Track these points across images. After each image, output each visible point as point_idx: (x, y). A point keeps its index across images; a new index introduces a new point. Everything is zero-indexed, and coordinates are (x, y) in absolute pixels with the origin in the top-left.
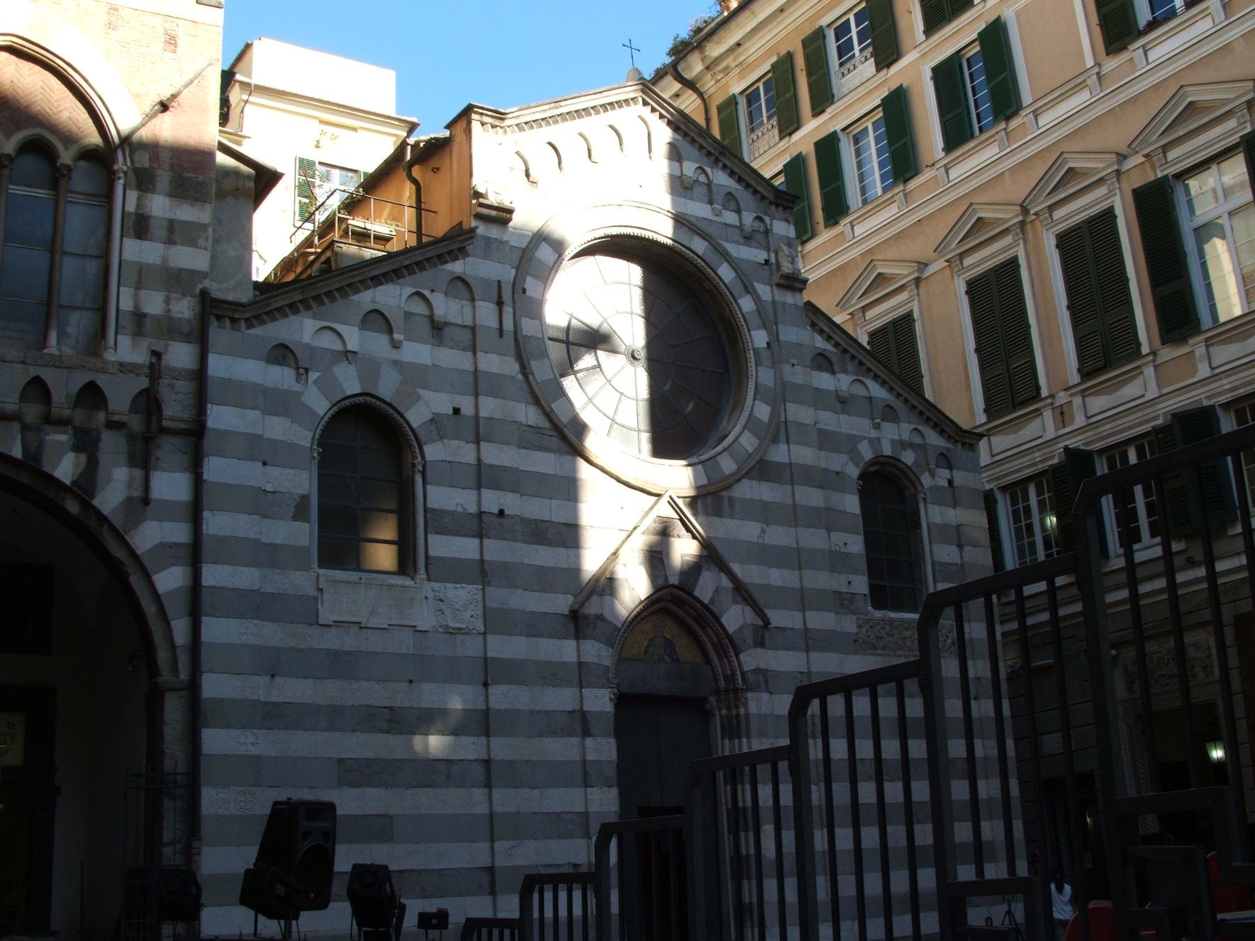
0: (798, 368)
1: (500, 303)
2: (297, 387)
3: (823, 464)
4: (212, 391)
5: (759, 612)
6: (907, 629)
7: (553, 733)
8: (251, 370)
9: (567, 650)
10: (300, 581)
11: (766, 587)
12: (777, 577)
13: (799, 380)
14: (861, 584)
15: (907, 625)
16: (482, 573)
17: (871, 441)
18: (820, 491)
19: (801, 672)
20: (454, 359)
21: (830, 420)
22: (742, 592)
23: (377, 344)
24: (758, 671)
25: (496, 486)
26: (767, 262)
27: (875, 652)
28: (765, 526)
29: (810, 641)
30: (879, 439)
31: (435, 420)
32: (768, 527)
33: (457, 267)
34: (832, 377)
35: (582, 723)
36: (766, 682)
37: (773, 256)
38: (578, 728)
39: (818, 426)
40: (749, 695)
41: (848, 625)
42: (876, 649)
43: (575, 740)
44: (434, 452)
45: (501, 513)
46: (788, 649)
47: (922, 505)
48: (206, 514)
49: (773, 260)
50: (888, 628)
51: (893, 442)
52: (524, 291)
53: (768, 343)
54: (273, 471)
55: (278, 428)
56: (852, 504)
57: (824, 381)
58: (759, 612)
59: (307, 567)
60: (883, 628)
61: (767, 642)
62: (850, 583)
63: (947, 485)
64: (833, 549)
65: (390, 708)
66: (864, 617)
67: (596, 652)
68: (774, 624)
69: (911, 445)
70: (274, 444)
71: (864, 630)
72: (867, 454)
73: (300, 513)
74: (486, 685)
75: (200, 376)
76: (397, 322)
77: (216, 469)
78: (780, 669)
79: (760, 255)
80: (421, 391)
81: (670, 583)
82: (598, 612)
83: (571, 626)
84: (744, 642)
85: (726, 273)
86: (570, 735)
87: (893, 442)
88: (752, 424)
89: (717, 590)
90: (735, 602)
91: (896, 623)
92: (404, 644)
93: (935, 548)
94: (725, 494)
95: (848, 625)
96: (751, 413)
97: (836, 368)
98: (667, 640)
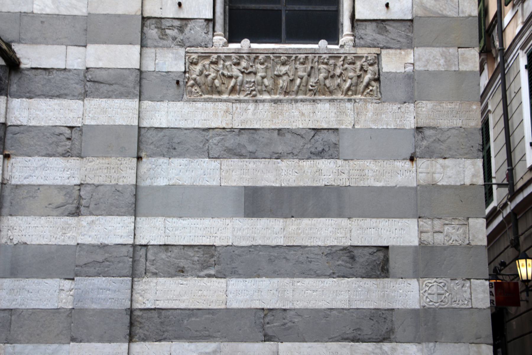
6: (284, 64)
15: (283, 58)
19: (71, 128)
27: (215, 97)
29: (88, 84)
42: (220, 93)
46: (52, 97)
50: (244, 64)
60: (237, 64)
61: (14, 88)
62: (180, 4)
66: (200, 50)
68: (25, 64)
71: (198, 68)
78: (33, 123)
91: (261, 57)
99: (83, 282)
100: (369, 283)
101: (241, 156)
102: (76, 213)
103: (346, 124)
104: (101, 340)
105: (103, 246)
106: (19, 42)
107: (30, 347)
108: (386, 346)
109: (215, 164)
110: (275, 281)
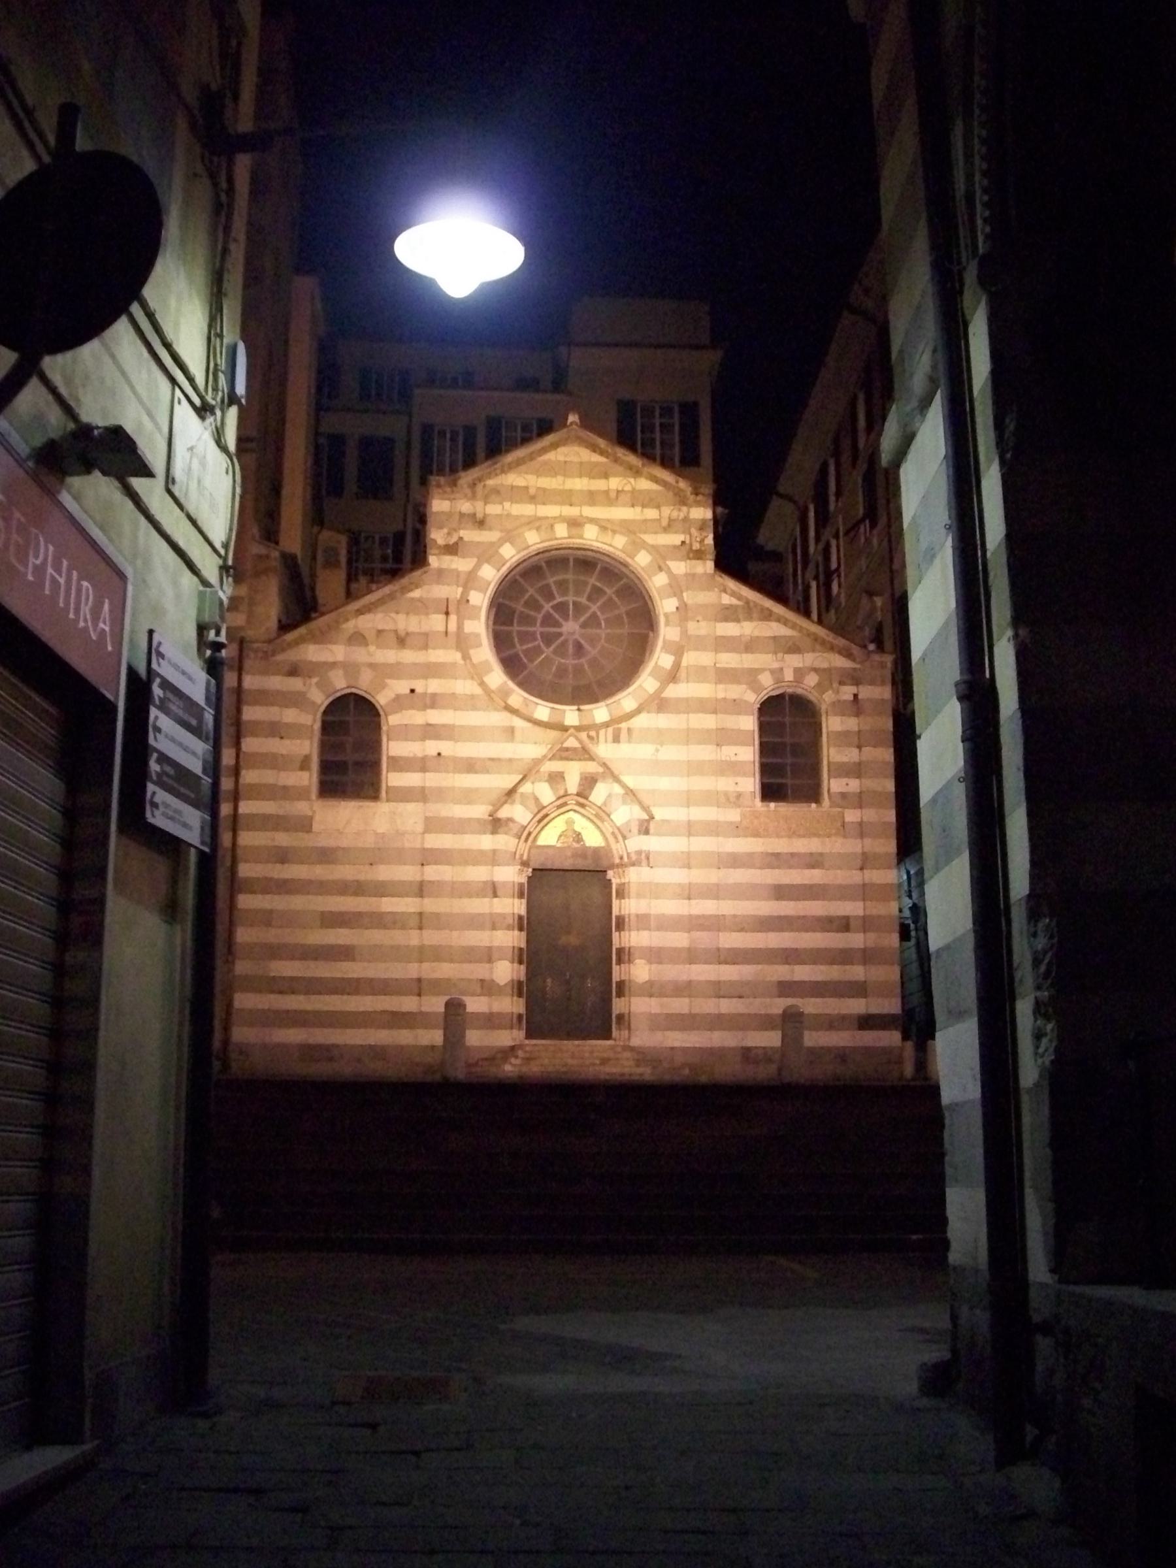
0: (703, 624)
1: (447, 613)
2: (303, 689)
3: (721, 695)
4: (244, 697)
5: (646, 809)
7: (470, 896)
8: (276, 682)
9: (486, 842)
10: (301, 808)
11: (653, 792)
12: (665, 783)
13: (703, 632)
14: (750, 784)
16: (421, 795)
17: (772, 672)
18: (714, 716)
20: (409, 656)
21: (729, 660)
22: (631, 794)
23: (360, 655)
24: (639, 853)
25: (437, 737)
26: (683, 543)
28: (659, 747)
30: (782, 669)
31: (398, 698)
32: (662, 746)
33: (416, 594)
34: (738, 625)
35: (494, 890)
36: (648, 859)
37: (688, 537)
38: (490, 893)
39: (717, 665)
40: (632, 869)
41: (734, 815)
43: (486, 900)
44: (392, 720)
45: (439, 754)
47: (824, 719)
48: (243, 772)
49: (688, 542)
51: (797, 671)
52: (468, 601)
53: (677, 608)
54: (287, 742)
55: (290, 715)
56: (749, 723)
57: (730, 629)
58: (646, 809)
59: (309, 799)
61: (652, 831)
62: (737, 783)
63: (851, 698)
64: (723, 759)
65: (357, 881)
67: (504, 842)
68: (658, 817)
69: (816, 670)
70: (288, 726)
72: (767, 680)
73: (304, 765)
74: (423, 865)
75: (239, 690)
76: (371, 636)
77: (250, 744)
79: (676, 539)
80: (388, 681)
81: (569, 792)
82: (509, 816)
83: (490, 827)
84: (630, 831)
85: (642, 560)
86: (484, 896)
87: (797, 671)
88: (656, 673)
89: (610, 796)
90: (624, 802)
92: (369, 842)
93: (832, 750)
94: (624, 725)
95: (734, 815)
96: (656, 663)
97: (741, 616)
98: (575, 832)
99: (697, 934)
100: (840, 935)
101: (773, 868)
102: (689, 899)
103: (827, 850)
104: (706, 963)
105: (703, 916)
106: (654, 806)
107: (669, 966)
108: (848, 967)
109: (758, 871)
110: (792, 934)
